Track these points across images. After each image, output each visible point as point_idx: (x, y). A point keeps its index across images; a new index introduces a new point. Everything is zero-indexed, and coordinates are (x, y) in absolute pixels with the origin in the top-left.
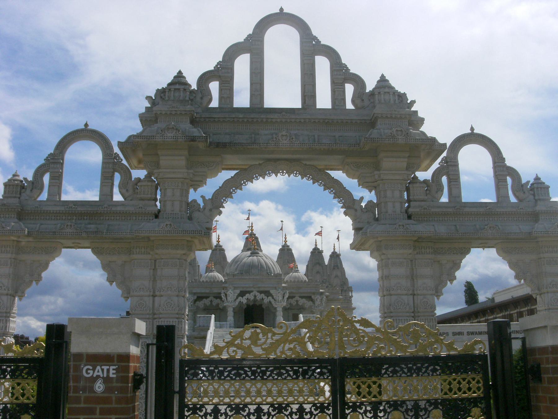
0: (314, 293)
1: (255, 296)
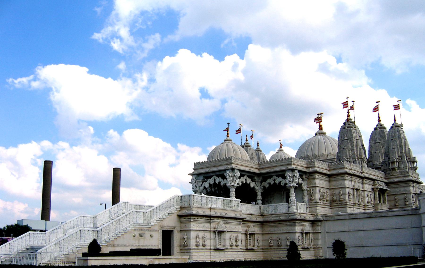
1: (215, 180)
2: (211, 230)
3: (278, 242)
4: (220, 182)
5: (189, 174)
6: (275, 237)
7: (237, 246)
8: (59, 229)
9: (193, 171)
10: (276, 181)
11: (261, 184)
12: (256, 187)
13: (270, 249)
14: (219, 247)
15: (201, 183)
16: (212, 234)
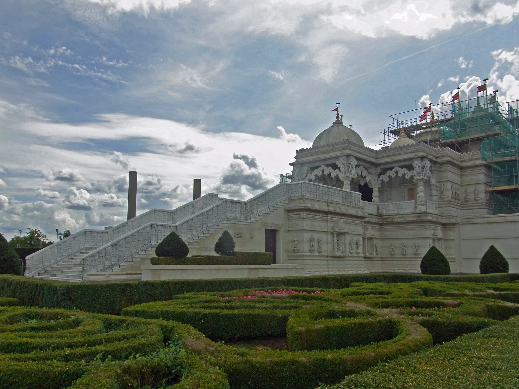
0: (411, 159)
1: (323, 171)
2: (329, 230)
3: (403, 249)
4: (330, 173)
5: (290, 164)
6: (398, 243)
7: (357, 253)
8: (126, 227)
9: (295, 160)
10: (398, 174)
11: (379, 177)
12: (372, 182)
13: (416, 258)
14: (338, 254)
15: (305, 175)
16: (330, 237)
